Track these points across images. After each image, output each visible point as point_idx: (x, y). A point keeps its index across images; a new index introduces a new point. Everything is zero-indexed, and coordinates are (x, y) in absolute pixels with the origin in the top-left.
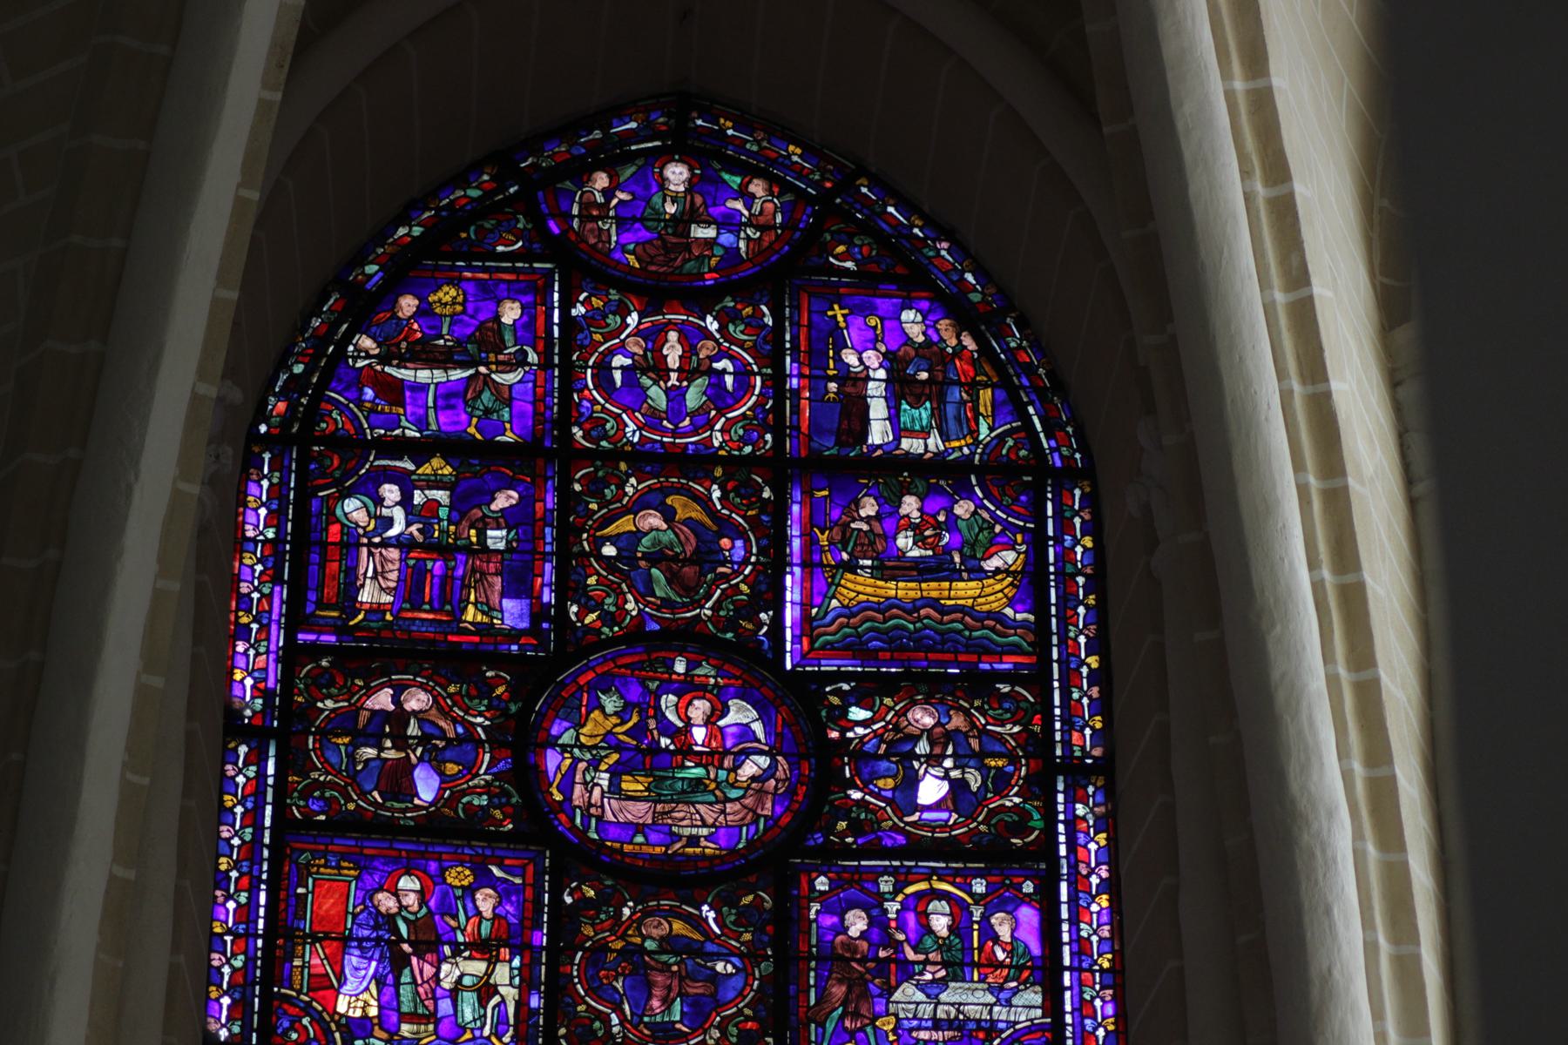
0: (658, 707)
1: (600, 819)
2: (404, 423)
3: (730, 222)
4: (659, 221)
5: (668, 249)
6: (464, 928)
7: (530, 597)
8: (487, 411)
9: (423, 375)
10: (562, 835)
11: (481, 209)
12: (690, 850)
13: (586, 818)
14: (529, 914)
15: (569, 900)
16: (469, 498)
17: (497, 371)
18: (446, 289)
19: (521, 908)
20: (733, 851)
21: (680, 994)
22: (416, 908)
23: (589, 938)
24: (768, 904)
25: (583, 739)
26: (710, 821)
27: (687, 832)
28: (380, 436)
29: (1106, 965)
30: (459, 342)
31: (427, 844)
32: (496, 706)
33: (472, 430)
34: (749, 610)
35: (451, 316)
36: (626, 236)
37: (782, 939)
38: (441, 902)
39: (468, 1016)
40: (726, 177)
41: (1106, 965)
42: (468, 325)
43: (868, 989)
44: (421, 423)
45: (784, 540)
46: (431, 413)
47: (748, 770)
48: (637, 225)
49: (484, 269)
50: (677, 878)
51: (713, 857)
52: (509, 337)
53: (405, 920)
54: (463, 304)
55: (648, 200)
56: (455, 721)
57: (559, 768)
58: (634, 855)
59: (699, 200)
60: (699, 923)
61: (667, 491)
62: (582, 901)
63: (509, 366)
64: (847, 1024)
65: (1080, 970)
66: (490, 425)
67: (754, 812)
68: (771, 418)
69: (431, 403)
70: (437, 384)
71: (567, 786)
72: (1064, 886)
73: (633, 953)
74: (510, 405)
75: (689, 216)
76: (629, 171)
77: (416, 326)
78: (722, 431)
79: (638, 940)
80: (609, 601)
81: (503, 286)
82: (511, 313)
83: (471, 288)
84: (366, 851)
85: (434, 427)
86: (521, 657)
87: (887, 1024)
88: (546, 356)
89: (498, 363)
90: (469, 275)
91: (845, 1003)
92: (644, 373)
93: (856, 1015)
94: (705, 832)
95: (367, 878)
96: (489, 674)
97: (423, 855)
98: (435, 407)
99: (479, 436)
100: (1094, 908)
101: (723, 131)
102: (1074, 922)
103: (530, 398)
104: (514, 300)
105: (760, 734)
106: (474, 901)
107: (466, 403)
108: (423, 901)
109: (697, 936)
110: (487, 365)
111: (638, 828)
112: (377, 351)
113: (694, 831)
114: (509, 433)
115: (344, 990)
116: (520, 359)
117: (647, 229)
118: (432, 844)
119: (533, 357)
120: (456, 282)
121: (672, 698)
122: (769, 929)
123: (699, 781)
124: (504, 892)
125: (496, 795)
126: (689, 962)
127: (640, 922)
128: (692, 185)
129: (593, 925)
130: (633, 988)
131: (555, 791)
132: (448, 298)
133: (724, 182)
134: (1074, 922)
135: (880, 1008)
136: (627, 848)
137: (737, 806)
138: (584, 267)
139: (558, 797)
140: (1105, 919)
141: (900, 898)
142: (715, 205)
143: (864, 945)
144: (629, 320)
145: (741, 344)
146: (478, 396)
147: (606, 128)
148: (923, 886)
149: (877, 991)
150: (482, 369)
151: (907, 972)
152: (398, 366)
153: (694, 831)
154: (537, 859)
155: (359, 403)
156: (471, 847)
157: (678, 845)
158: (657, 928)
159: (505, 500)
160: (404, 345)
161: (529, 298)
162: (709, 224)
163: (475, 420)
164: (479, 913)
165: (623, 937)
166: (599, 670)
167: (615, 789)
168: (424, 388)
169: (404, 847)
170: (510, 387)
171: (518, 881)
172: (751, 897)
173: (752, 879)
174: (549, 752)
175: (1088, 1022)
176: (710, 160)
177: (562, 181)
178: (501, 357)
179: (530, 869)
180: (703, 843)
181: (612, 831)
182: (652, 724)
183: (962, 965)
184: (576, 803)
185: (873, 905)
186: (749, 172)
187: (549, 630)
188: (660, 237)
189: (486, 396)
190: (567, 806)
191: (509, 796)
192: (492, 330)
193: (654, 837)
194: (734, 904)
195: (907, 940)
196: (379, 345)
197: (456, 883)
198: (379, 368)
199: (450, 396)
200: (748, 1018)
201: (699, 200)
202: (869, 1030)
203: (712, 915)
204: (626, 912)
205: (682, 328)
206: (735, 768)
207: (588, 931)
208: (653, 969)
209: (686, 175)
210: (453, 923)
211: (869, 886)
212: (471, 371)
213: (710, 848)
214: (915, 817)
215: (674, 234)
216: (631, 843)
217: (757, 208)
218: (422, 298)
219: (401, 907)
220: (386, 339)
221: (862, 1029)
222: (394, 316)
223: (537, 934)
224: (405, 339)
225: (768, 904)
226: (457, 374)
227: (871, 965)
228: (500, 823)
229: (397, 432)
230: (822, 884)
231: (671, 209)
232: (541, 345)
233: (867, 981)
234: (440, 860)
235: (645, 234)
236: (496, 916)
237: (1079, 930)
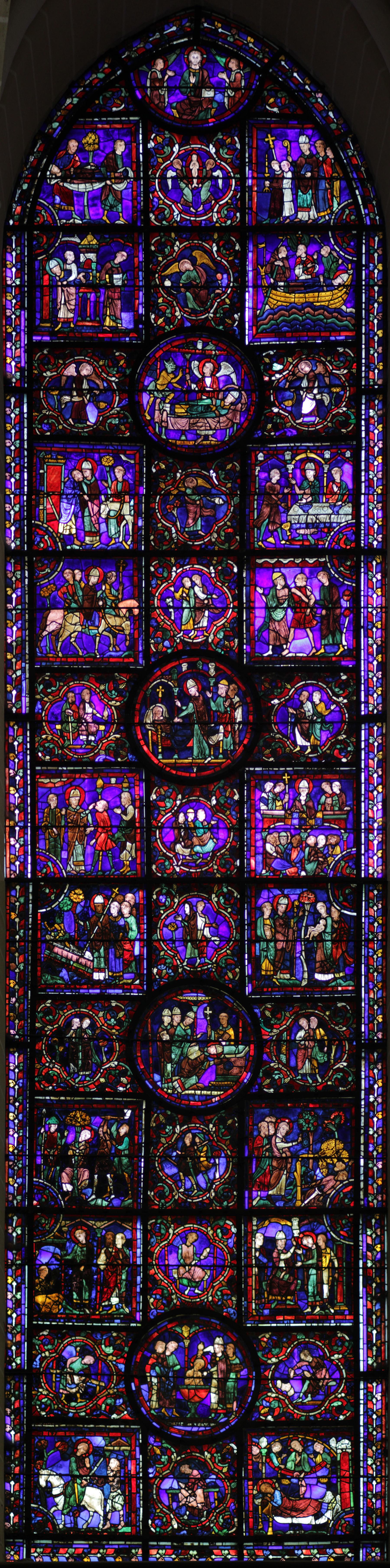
0: (190, 368)
1: (166, 428)
3: (220, 87)
4: (187, 88)
5: (192, 105)
6: (111, 487)
7: (133, 311)
10: (150, 437)
11: (106, 85)
12: (205, 442)
13: (161, 428)
14: (137, 479)
15: (154, 470)
16: (105, 256)
19: (134, 476)
20: (223, 442)
21: (200, 516)
22: (90, 478)
23: (163, 489)
24: (238, 469)
25: (158, 387)
26: (213, 427)
27: (203, 433)
29: (380, 492)
31: (93, 445)
32: (121, 372)
34: (229, 313)
36: (173, 98)
37: (244, 485)
38: (101, 474)
39: (113, 532)
40: (218, 58)
41: (380, 492)
43: (279, 509)
45: (244, 273)
47: (230, 399)
48: (177, 91)
50: (198, 457)
51: (215, 445)
53: (86, 484)
55: (182, 75)
56: (103, 380)
57: (148, 402)
58: (181, 446)
59: (206, 74)
60: (208, 479)
61: (193, 248)
62: (160, 470)
64: (270, 527)
65: (368, 494)
66: (114, 216)
67: (231, 420)
68: (239, 205)
71: (152, 413)
72: (363, 453)
73: (181, 495)
75: (201, 85)
76: (173, 58)
78: (217, 212)
79: (183, 489)
80: (168, 311)
84: (68, 450)
86: (131, 344)
87: (286, 527)
91: (269, 517)
92: (181, 181)
93: (274, 523)
94: (211, 432)
95: (69, 463)
96: (117, 354)
97: (93, 451)
100: (376, 463)
101: (216, 30)
102: (367, 471)
105: (235, 380)
106: (114, 473)
108: (93, 474)
109: (208, 486)
111: (183, 432)
113: (207, 432)
115: (62, 520)
116: (125, 176)
117: (182, 93)
118: (96, 445)
121: (196, 363)
122: (238, 481)
123: (208, 406)
124: (127, 467)
125: (122, 418)
126: (204, 499)
127: (184, 480)
128: (203, 64)
129: (164, 483)
130: (181, 514)
131: (146, 414)
133: (217, 62)
134: (367, 471)
135: (284, 519)
136: (178, 443)
137: (225, 419)
138: (153, 119)
139: (148, 418)
140: (380, 468)
141: (294, 462)
142: (213, 77)
143: (278, 487)
144: (174, 149)
145: (225, 160)
147: (161, 31)
148: (303, 456)
149: (282, 510)
151: (295, 499)
153: (207, 432)
154: (140, 450)
156: (112, 446)
157: (200, 440)
158: (191, 483)
159: (121, 257)
162: (210, 88)
164: (116, 479)
165: (177, 488)
166: (165, 349)
167: (172, 412)
169: (84, 447)
171: (132, 462)
172: (230, 465)
173: (231, 456)
174: (144, 394)
175: (371, 521)
176: (210, 45)
177: (141, 66)
179: (138, 455)
180: (211, 438)
181: (172, 435)
182: (188, 377)
183: (319, 494)
184: (156, 420)
185: (282, 466)
186: (229, 55)
187: (142, 329)
188: (188, 98)
190: (152, 422)
191: (128, 418)
193: (189, 436)
194: (223, 469)
195: (296, 484)
197: (107, 464)
199: (96, 198)
200: (229, 527)
201: (206, 74)
202: (279, 530)
203: (214, 475)
204: (178, 475)
205: (199, 152)
206: (223, 399)
207: (163, 486)
208: (189, 503)
209: (199, 59)
210: (106, 485)
211: (280, 457)
213: (213, 441)
214: (300, 421)
215: (194, 96)
216: (180, 440)
217: (233, 77)
219: (84, 478)
221: (276, 530)
223: (141, 488)
225: (238, 469)
227: (280, 496)
228: (124, 433)
230: (261, 457)
231: (193, 80)
233: (278, 505)
234: (99, 453)
235: (181, 97)
236: (124, 480)
237: (369, 475)
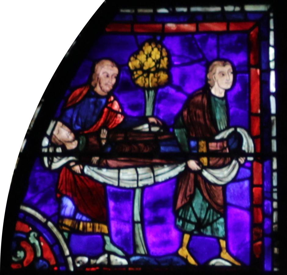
2: (109, 247)
8: (200, 224)
9: (128, 177)
17: (210, 167)
18: (148, 49)
28: (84, 266)
30: (165, 126)
33: (184, 252)
35: (156, 88)
42: (174, 101)
44: (127, 246)
46: (138, 228)
49: (190, 18)
52: (220, 116)
54: (167, 71)
63: (221, 159)
69: (137, 217)
70: (143, 188)
74: (224, 215)
77: (116, 106)
81: (212, 41)
82: (222, 80)
83: (175, 44)
85: (142, 250)
88: (262, 140)
89: (210, 154)
90: (171, 26)
98: (142, 222)
99: (191, 261)
103: (246, 203)
104: (225, 61)
107: (176, 213)
110: (197, 157)
112: (73, 146)
114: (225, 254)
119: (248, 144)
120: (159, 38)
132: (150, 64)
146: (189, 204)
150: (193, 164)
152: (100, 166)
155: (58, 219)
160: (104, 134)
161: (240, 58)
163: (186, 237)
168: (129, 194)
170: (224, 187)
178: (213, 146)
189: (198, 202)
192: (200, 106)
196: (77, 137)
198: (77, 169)
212: (180, 168)
218: (122, 65)
220: (84, 127)
222: (92, 93)
224: (105, 126)
226: (166, 173)
229: (102, 259)
232: (256, 125)
